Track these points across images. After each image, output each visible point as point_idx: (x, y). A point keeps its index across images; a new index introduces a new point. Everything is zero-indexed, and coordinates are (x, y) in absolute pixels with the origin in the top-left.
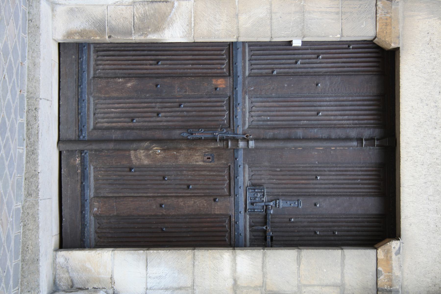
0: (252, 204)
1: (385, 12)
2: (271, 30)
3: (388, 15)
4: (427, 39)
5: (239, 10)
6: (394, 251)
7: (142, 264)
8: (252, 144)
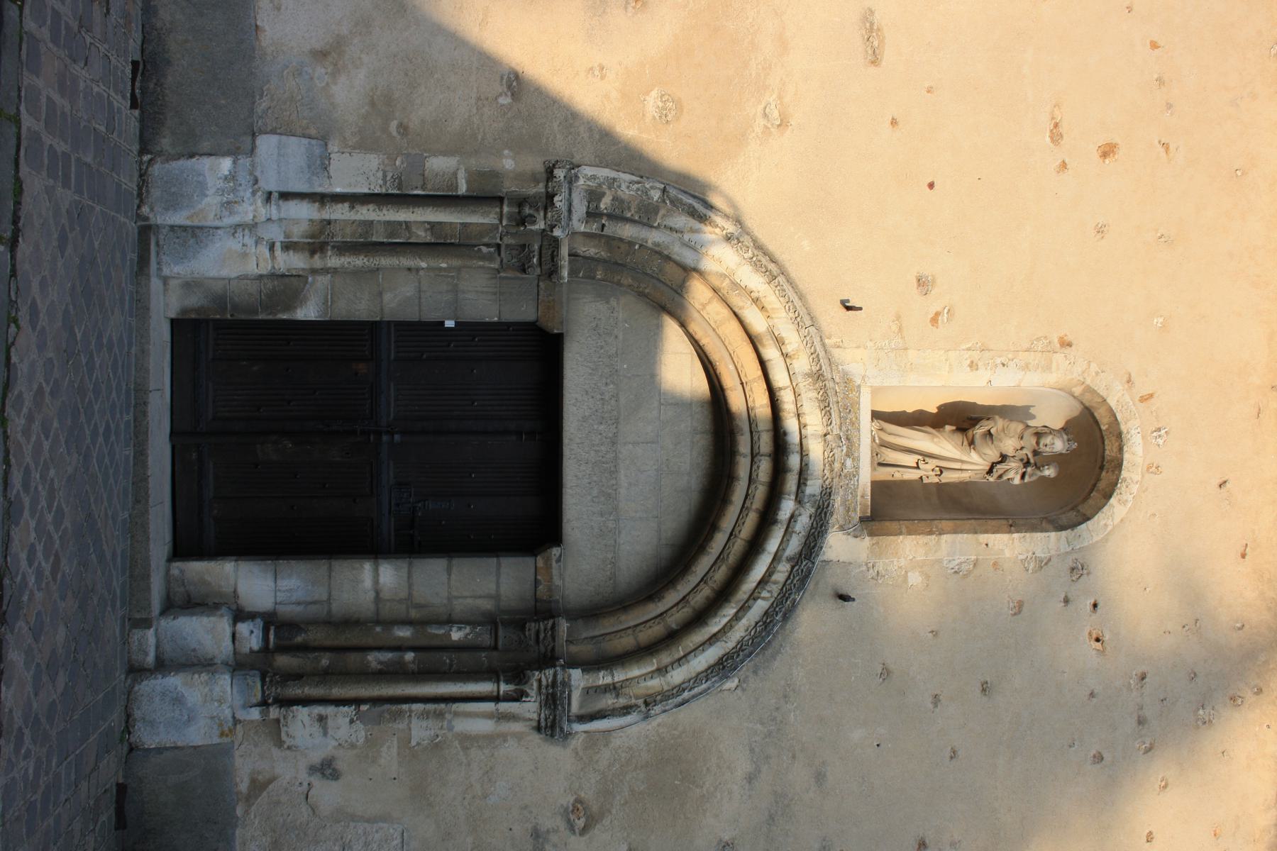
0: (398, 505)
2: (420, 311)
4: (594, 324)
6: (554, 559)
7: (270, 576)
8: (397, 437)
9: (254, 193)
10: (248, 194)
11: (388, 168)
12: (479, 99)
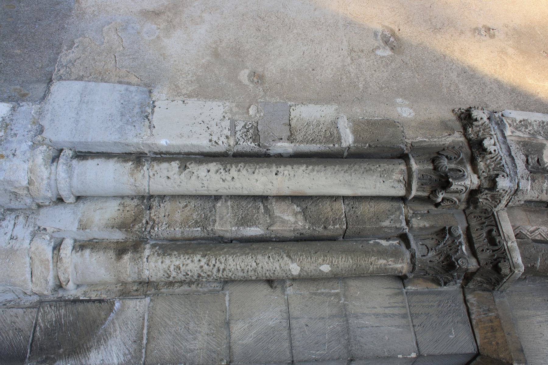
1: (484, 310)
2: (291, 347)
3: (492, 314)
5: (231, 315)
9: (33, 147)
10: (25, 146)
11: (237, 117)
12: (352, 50)
